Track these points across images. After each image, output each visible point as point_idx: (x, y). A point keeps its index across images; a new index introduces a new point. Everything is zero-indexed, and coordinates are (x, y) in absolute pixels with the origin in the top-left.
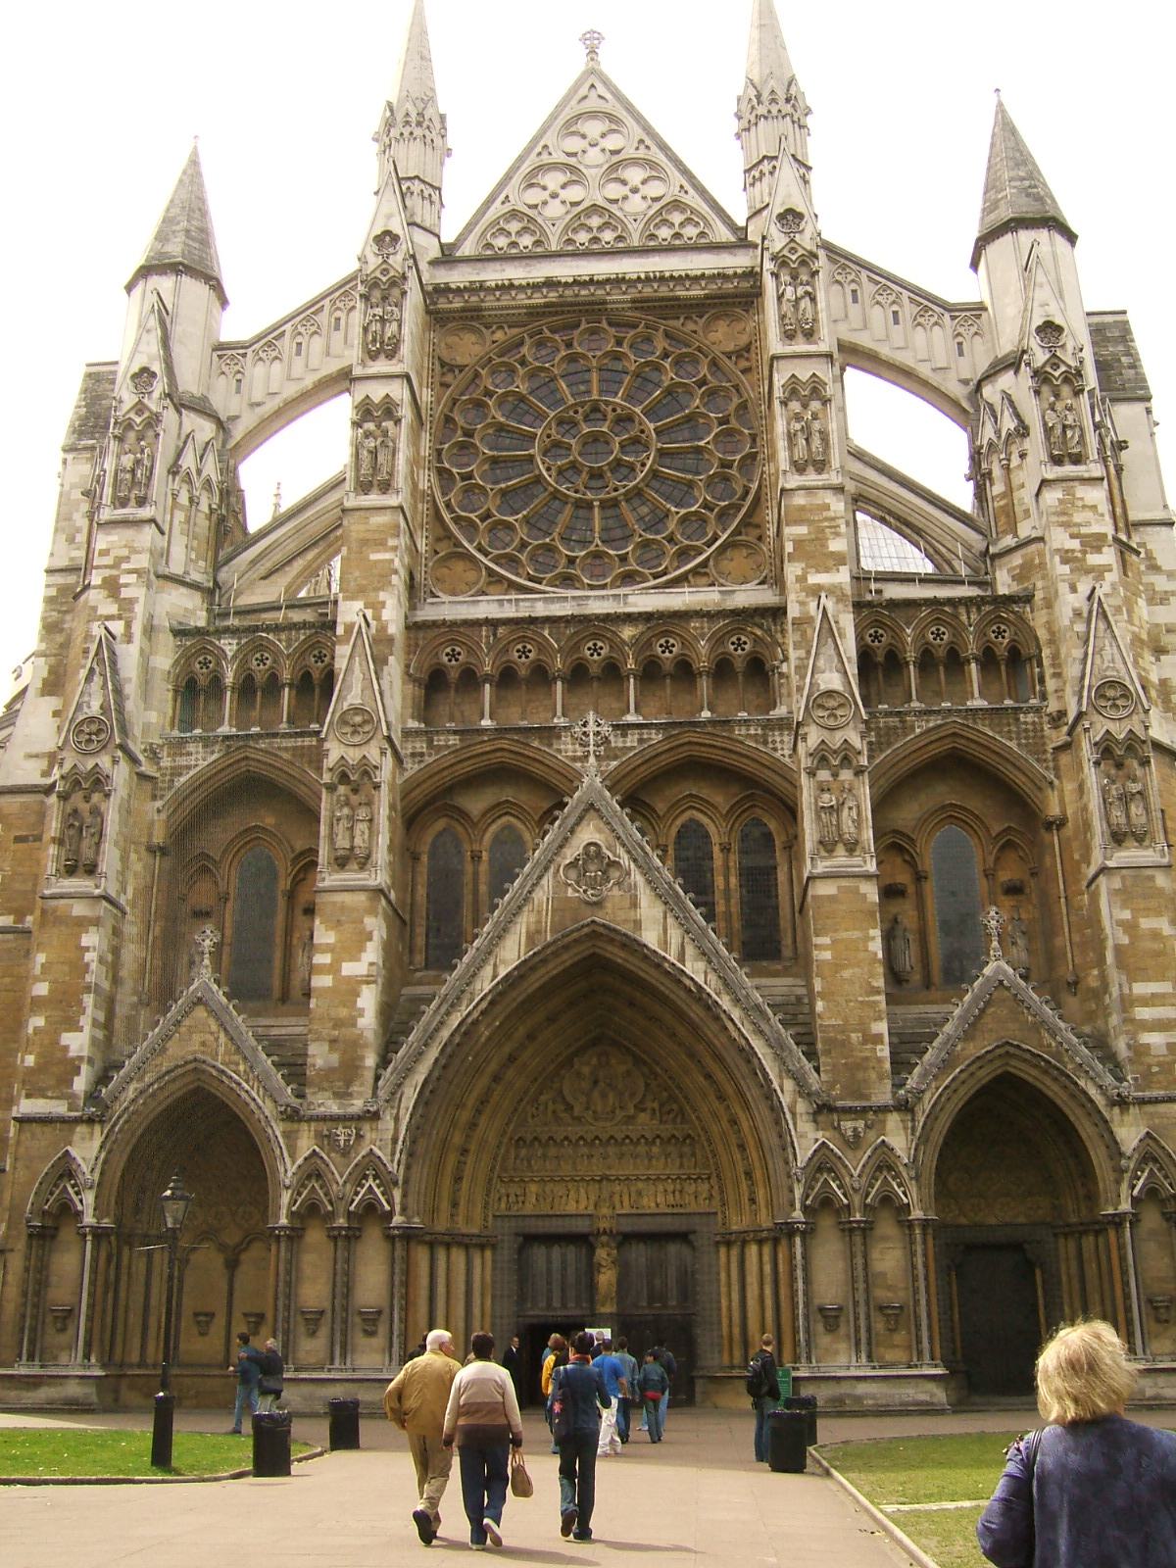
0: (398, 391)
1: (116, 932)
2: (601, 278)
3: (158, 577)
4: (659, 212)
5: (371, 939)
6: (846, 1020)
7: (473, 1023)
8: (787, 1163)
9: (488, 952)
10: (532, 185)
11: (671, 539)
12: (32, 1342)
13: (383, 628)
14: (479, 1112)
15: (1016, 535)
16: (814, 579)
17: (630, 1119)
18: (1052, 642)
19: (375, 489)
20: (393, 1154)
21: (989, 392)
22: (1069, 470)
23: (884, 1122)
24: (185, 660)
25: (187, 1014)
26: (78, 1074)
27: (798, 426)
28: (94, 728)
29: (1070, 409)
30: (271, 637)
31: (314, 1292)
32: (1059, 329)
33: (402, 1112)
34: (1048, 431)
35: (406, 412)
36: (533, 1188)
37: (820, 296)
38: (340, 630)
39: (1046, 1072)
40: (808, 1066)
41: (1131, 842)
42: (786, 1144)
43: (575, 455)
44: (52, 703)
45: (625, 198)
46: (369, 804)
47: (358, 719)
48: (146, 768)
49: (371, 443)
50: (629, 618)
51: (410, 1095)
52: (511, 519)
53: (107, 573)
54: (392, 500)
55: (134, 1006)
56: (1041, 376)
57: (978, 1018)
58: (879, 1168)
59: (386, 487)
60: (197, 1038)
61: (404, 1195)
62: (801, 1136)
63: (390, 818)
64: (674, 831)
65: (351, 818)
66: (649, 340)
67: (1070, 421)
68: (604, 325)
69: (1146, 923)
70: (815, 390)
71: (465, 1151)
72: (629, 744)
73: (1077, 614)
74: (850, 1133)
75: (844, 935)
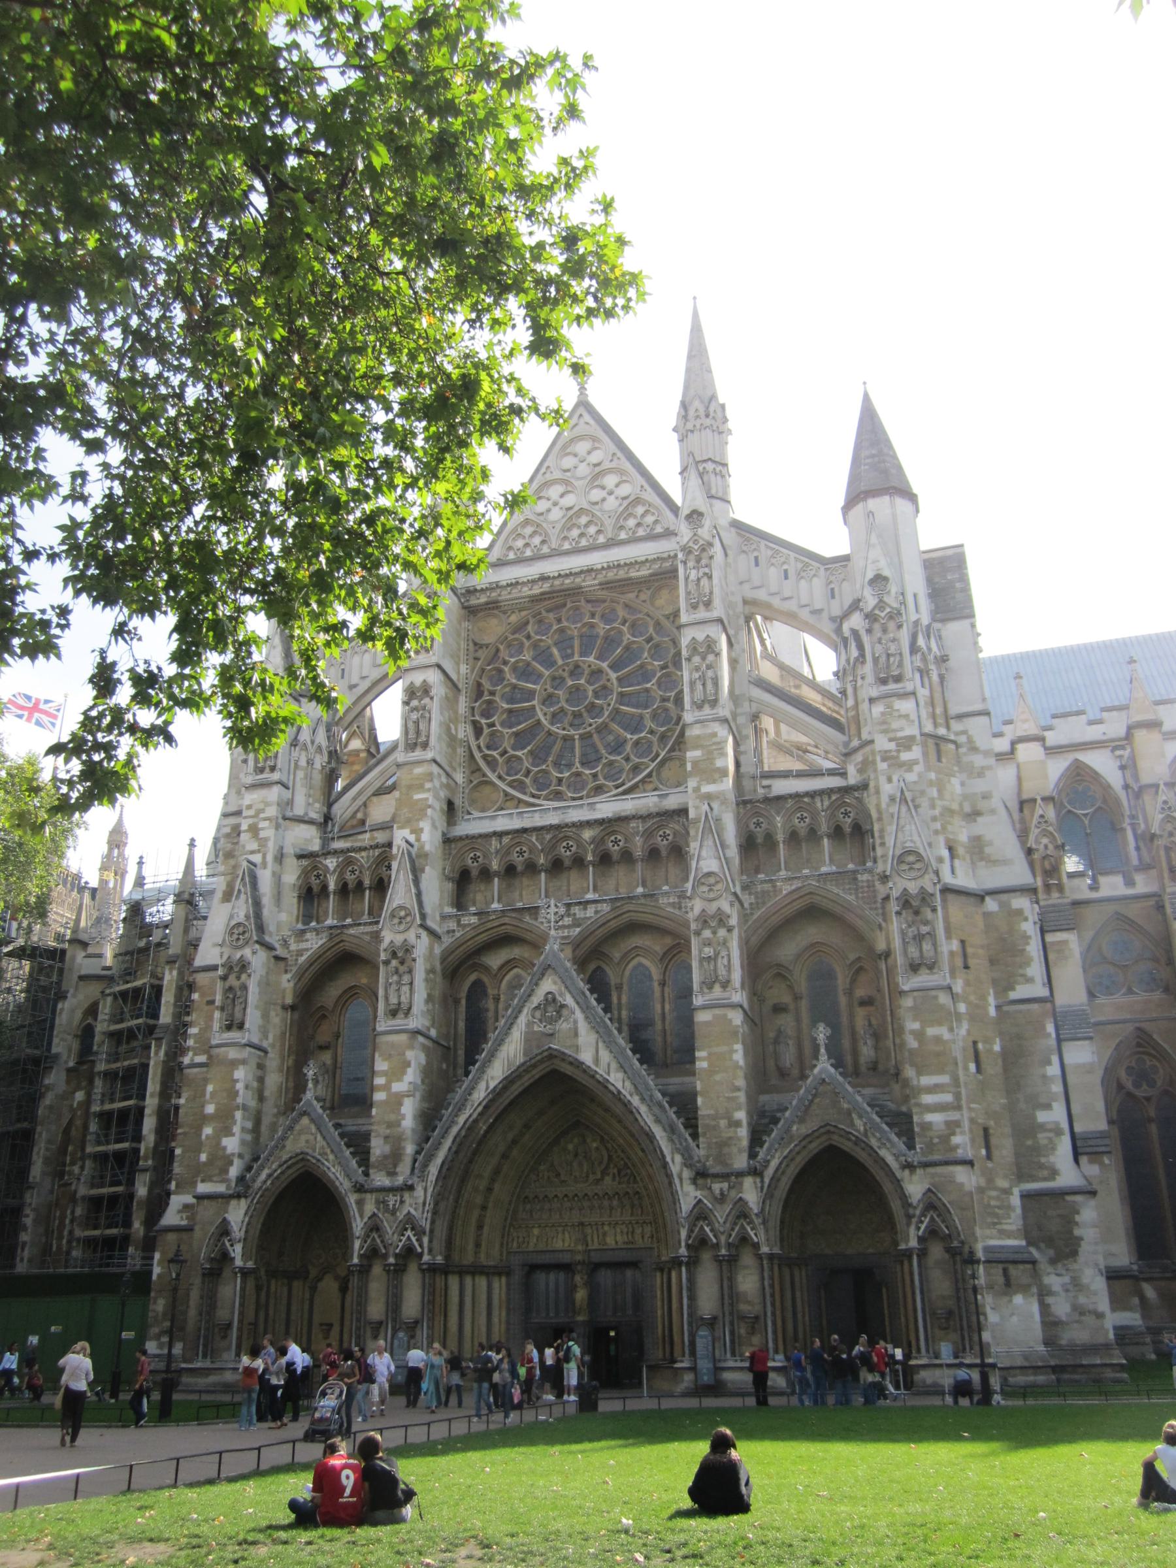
0: (433, 677)
1: (260, 1066)
3: (285, 818)
4: (627, 508)
5: (409, 1065)
9: (482, 1070)
10: (539, 498)
11: (627, 759)
12: (205, 1346)
13: (422, 847)
14: (493, 1180)
15: (860, 738)
16: (707, 788)
17: (597, 1182)
18: (880, 819)
19: (419, 748)
21: (846, 627)
22: (892, 686)
23: (741, 1184)
24: (305, 873)
25: (296, 1121)
26: (231, 1163)
27: (696, 675)
28: (241, 929)
29: (894, 640)
31: (376, 1309)
32: (886, 579)
34: (876, 660)
35: (439, 690)
36: (536, 1231)
37: (715, 575)
38: (395, 850)
39: (856, 1144)
41: (924, 970)
42: (675, 1201)
43: (563, 704)
44: (229, 906)
45: (604, 500)
46: (410, 971)
47: (402, 913)
48: (280, 952)
49: (414, 716)
50: (589, 824)
51: (433, 1170)
52: (519, 753)
53: (250, 821)
54: (429, 755)
55: (276, 1115)
56: (871, 617)
57: (808, 1108)
58: (738, 1217)
59: (425, 745)
60: (303, 1138)
61: (430, 1241)
62: (686, 1194)
63: (427, 980)
64: (627, 973)
65: (399, 983)
66: (613, 610)
67: (892, 650)
68: (583, 603)
69: (931, 1031)
70: (709, 647)
71: (484, 1208)
73: (892, 799)
74: (717, 1192)
75: (716, 1049)
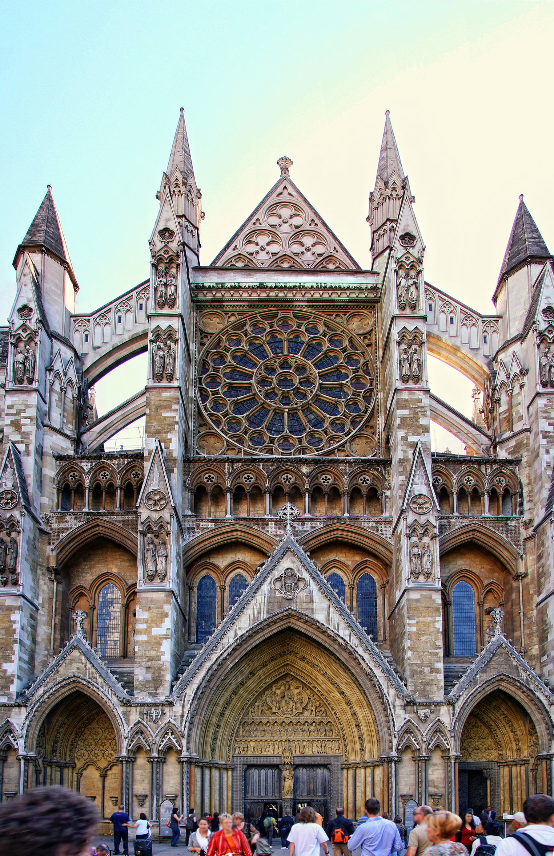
2: (291, 285)
5: (166, 615)
6: (423, 662)
7: (224, 659)
8: (389, 729)
20: (181, 723)
30: (109, 462)
33: (186, 702)
40: (402, 684)
50: (305, 462)
51: (190, 693)
58: (436, 731)
61: (188, 743)
62: (398, 716)
72: (305, 529)
74: (422, 715)
